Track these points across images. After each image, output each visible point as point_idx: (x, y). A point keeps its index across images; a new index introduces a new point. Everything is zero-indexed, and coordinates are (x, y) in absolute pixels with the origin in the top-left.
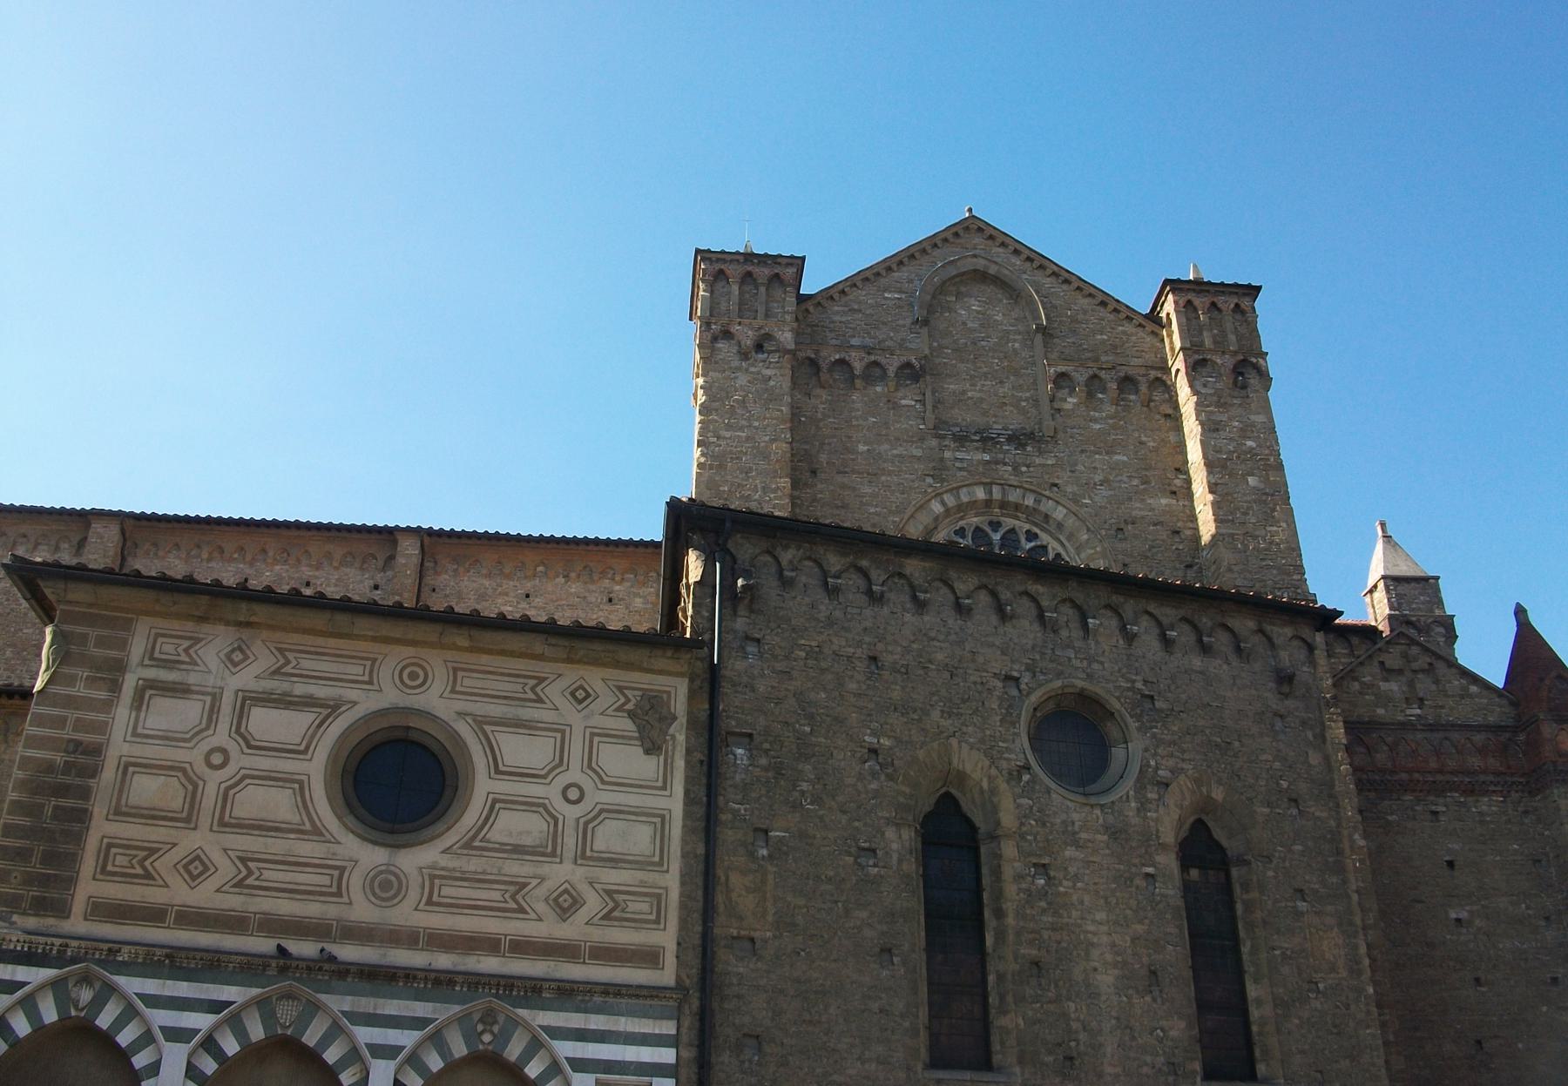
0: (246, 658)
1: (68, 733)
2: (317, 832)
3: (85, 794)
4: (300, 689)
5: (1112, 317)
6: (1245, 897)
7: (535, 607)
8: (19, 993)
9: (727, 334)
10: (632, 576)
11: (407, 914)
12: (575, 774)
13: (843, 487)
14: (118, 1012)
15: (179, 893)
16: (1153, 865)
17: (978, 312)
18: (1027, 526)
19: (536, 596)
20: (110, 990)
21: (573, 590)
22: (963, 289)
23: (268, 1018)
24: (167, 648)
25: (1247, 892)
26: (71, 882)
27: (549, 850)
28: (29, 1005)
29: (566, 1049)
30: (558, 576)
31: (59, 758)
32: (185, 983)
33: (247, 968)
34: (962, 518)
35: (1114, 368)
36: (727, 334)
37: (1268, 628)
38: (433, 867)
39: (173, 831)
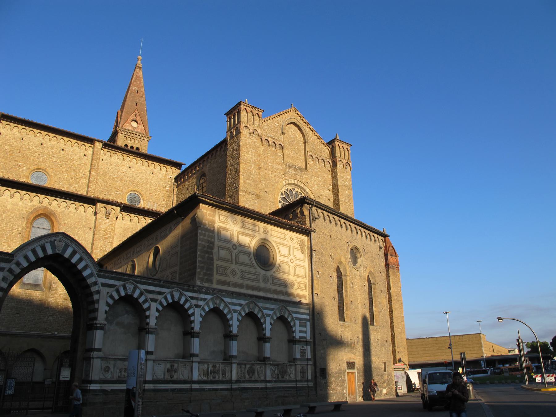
2: (253, 266)
3: (212, 254)
6: (374, 291)
12: (292, 257)
13: (266, 173)
14: (32, 283)
15: (231, 279)
16: (365, 284)
17: (293, 133)
18: (300, 191)
19: (132, 168)
21: (143, 168)
23: (249, 308)
25: (375, 290)
26: (212, 275)
28: (207, 304)
29: (295, 315)
31: (206, 244)
32: (235, 300)
33: (246, 296)
34: (287, 186)
35: (320, 156)
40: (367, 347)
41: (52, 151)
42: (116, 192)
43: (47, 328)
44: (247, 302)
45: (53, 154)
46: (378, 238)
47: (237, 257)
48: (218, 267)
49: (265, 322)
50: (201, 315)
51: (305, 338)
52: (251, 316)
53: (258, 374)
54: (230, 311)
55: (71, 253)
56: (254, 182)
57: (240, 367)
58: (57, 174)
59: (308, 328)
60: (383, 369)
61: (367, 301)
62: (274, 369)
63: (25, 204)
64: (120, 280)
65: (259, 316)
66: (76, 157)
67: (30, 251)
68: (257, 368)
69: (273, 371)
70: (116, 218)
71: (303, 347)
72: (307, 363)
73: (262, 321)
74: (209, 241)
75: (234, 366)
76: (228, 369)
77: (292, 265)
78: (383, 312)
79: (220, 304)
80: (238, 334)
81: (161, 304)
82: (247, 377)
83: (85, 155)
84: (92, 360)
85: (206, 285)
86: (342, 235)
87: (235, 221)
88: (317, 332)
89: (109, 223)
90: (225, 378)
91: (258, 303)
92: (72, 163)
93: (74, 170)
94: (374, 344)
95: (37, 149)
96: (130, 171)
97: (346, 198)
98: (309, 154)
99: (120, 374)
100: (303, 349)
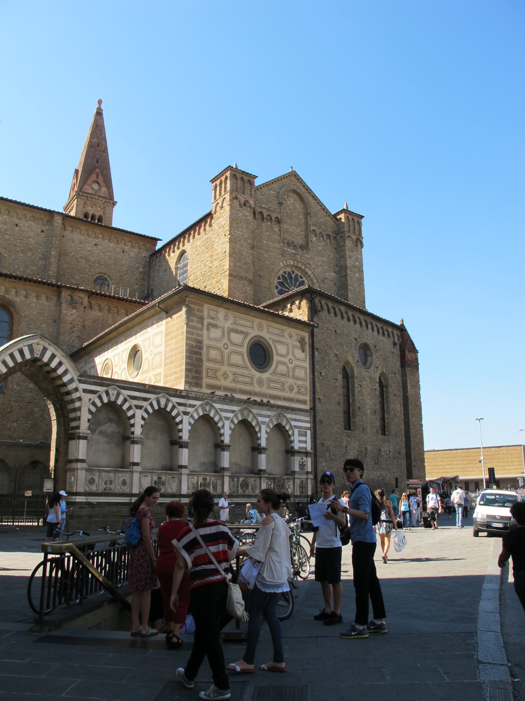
0: (228, 318)
1: (195, 337)
3: (201, 354)
4: (240, 328)
5: (325, 214)
8: (195, 408)
9: (236, 198)
11: (265, 390)
12: (290, 356)
13: (260, 253)
15: (222, 382)
17: (293, 203)
18: (300, 274)
20: (212, 406)
22: (289, 194)
23: (242, 414)
24: (212, 314)
26: (201, 378)
27: (286, 375)
28: (196, 410)
29: (293, 423)
30: (106, 239)
33: (240, 402)
34: (286, 269)
36: (236, 198)
37: (393, 331)
38: (268, 378)
39: (219, 366)
40: (376, 460)
41: (4, 227)
42: (81, 275)
43: (12, 436)
44: (240, 408)
45: (6, 231)
46: (392, 332)
47: (229, 358)
48: (208, 369)
49: (260, 430)
50: (190, 423)
51: (306, 448)
52: (245, 424)
53: (252, 489)
54: (221, 419)
55: (50, 357)
56: (245, 264)
57: (233, 480)
58: (11, 254)
59: (309, 438)
60: (395, 486)
61: (378, 407)
62: (270, 483)
64: (102, 385)
65: (254, 424)
66: (32, 234)
67: (8, 356)
68: (251, 481)
69: (269, 485)
71: (302, 459)
72: (307, 476)
73: (257, 429)
74: (197, 340)
75: (227, 480)
76: (219, 482)
77: (291, 366)
78: (396, 420)
79: (210, 410)
80: (230, 444)
81: (146, 411)
82: (240, 491)
83: (42, 231)
84: (76, 471)
85: (195, 389)
86: (350, 329)
87: (226, 317)
88: (318, 442)
89: (75, 313)
90: (217, 492)
91: (252, 410)
92: (29, 241)
93: (31, 249)
94: (384, 456)
97: (355, 282)
98: (312, 228)
99: (105, 486)
100: (302, 461)
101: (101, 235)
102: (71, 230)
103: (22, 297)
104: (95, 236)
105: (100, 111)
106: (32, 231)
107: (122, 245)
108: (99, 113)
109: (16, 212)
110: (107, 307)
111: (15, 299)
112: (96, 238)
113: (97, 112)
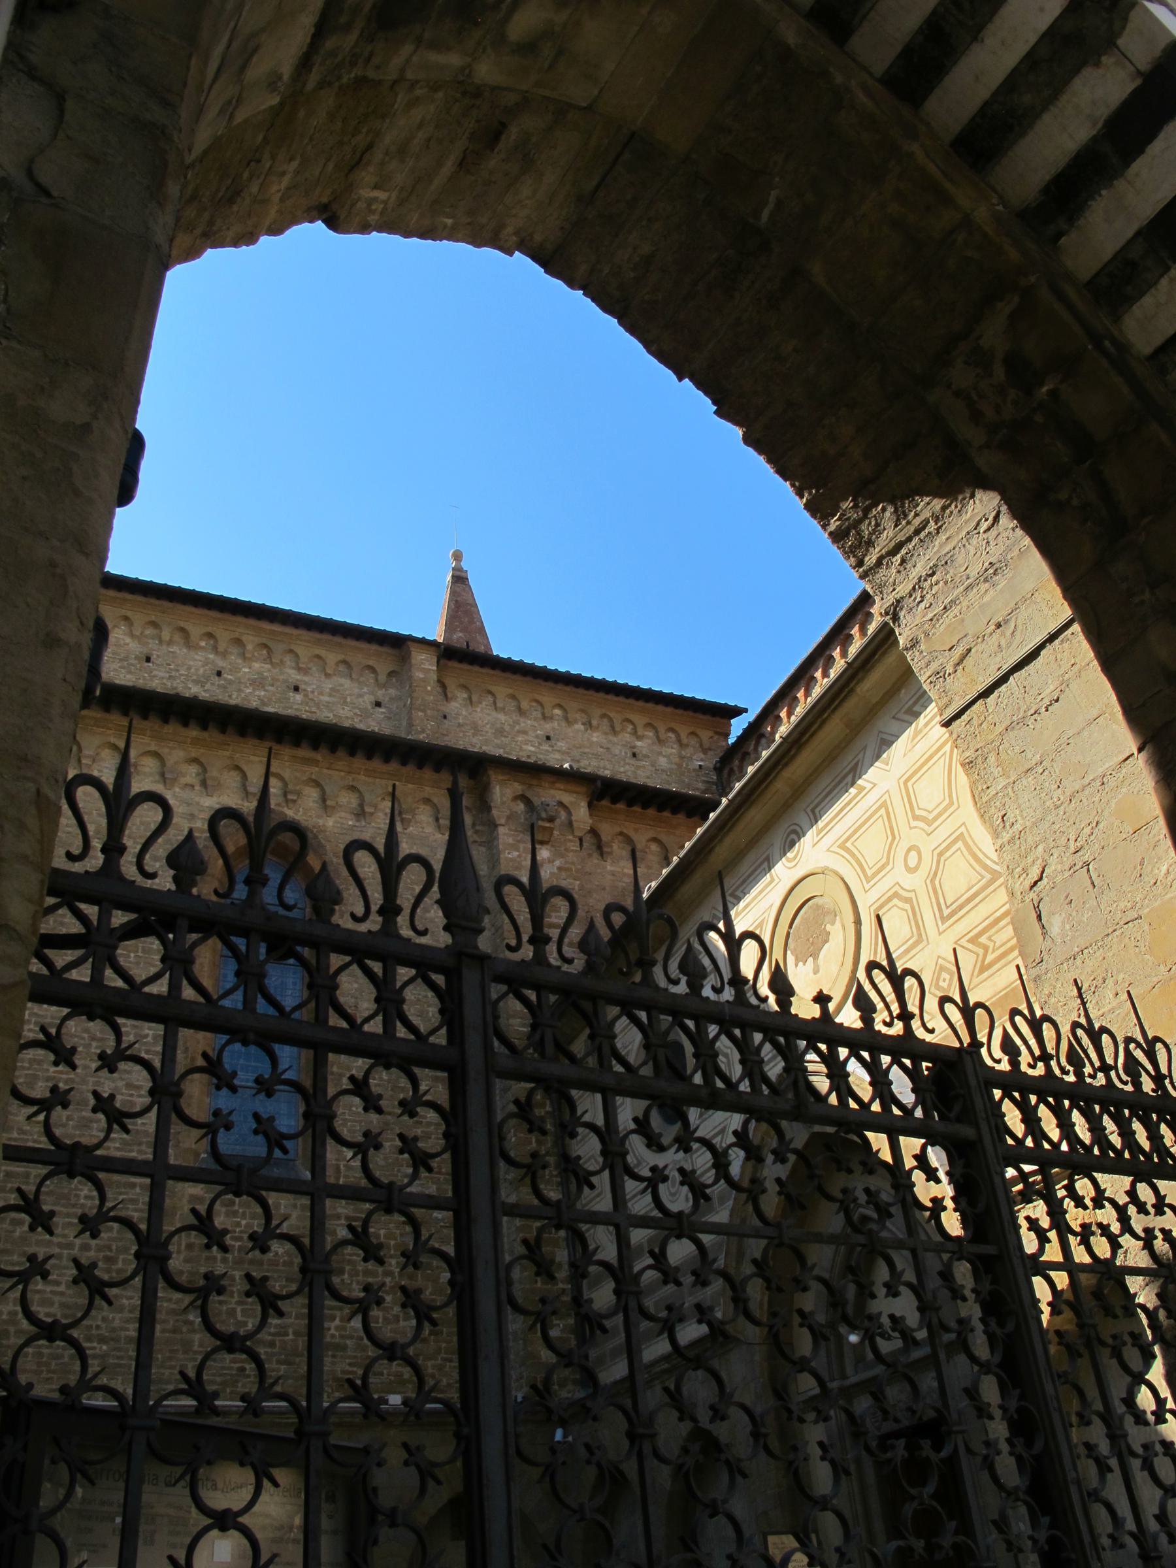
7: (559, 751)
10: (651, 734)
19: (558, 740)
21: (595, 739)
30: (576, 722)
41: (257, 693)
63: (189, 804)
70: (577, 839)
95: (205, 691)
96: (550, 749)
101: (557, 712)
102: (464, 699)
103: (343, 814)
104: (543, 714)
105: (463, 574)
106: (345, 703)
107: (627, 737)
108: (460, 579)
109: (291, 651)
110: (654, 847)
111: (321, 822)
112: (544, 717)
113: (453, 576)
